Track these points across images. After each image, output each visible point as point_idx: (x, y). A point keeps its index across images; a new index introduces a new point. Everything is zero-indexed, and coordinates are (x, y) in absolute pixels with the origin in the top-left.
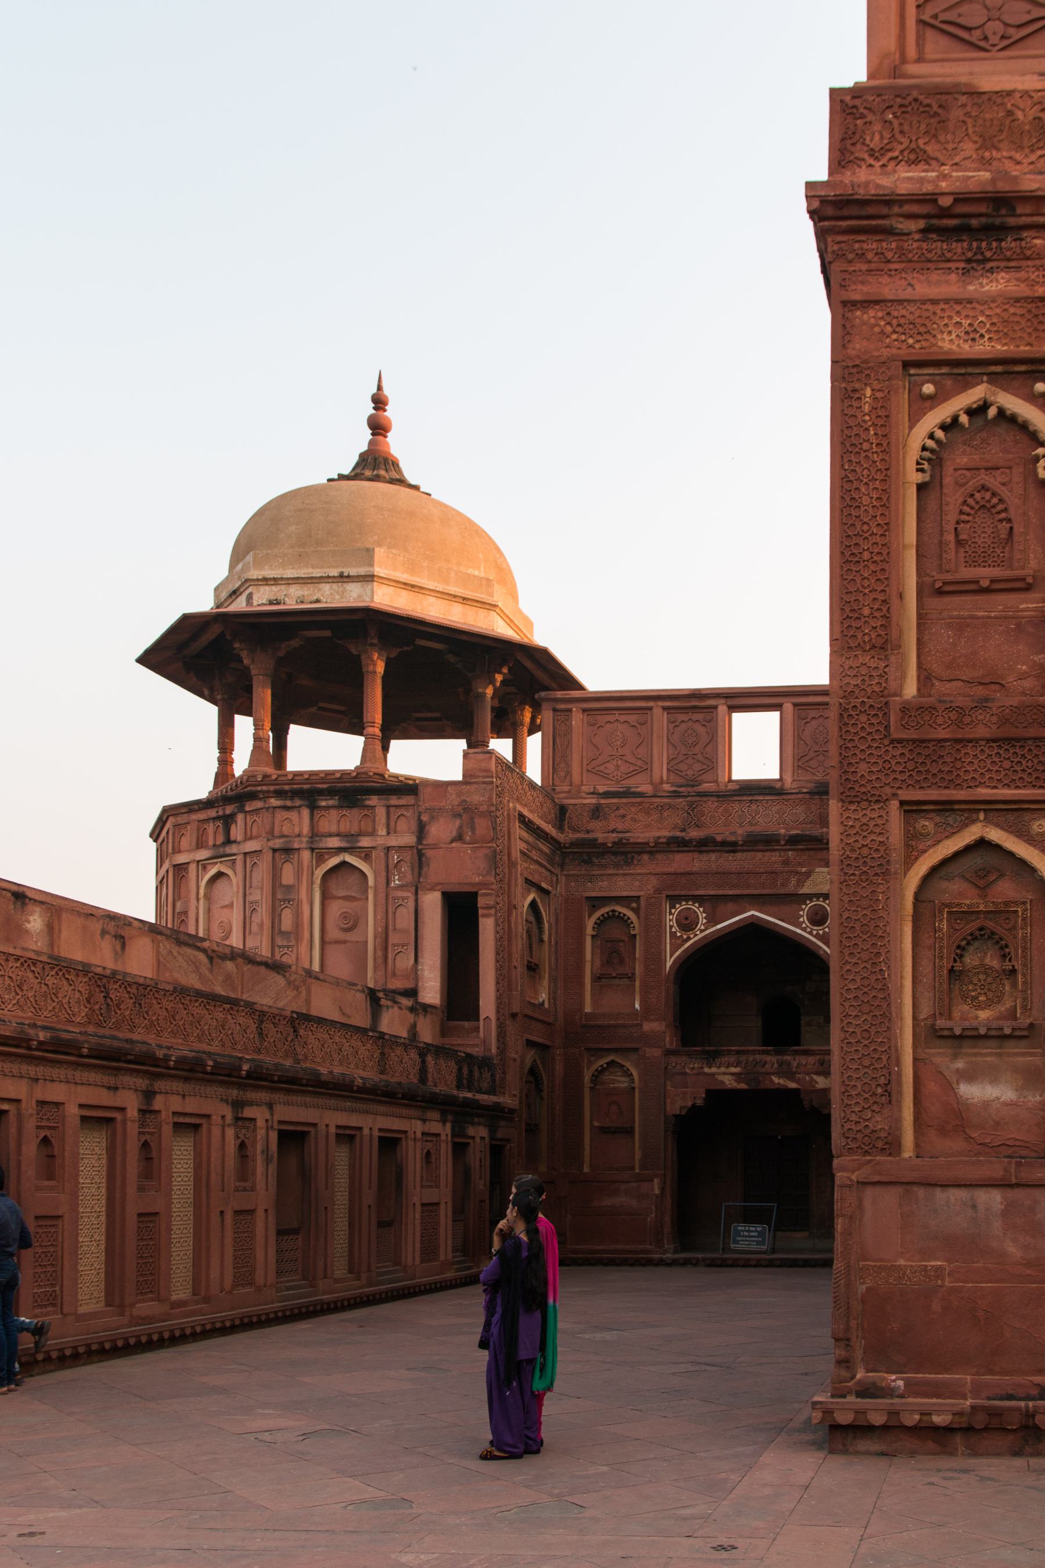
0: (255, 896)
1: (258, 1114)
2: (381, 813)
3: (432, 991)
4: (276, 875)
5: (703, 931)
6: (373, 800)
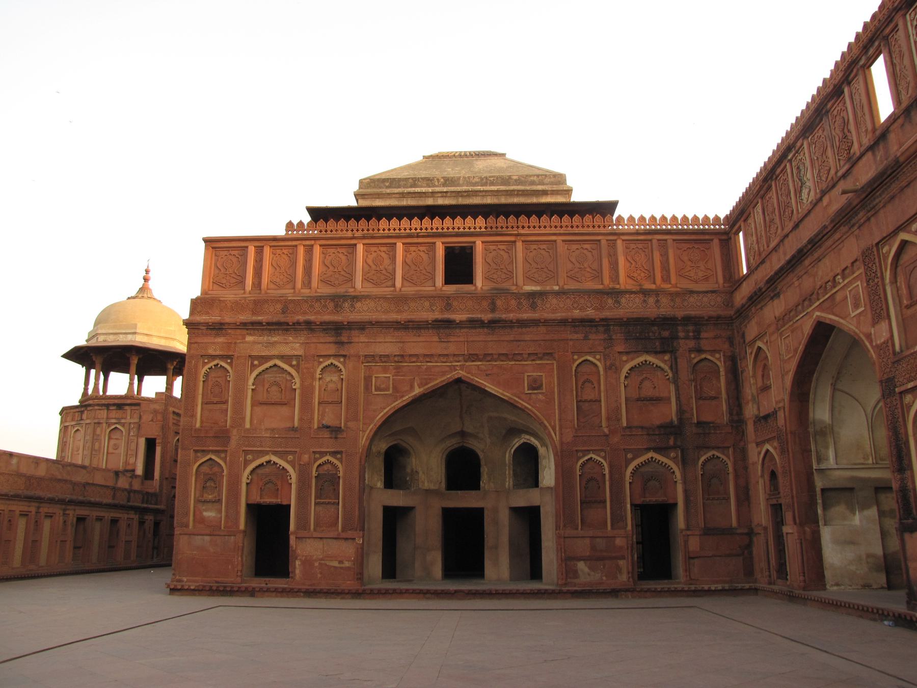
0: (88, 438)
1: (71, 513)
2: (129, 412)
6: (127, 407)
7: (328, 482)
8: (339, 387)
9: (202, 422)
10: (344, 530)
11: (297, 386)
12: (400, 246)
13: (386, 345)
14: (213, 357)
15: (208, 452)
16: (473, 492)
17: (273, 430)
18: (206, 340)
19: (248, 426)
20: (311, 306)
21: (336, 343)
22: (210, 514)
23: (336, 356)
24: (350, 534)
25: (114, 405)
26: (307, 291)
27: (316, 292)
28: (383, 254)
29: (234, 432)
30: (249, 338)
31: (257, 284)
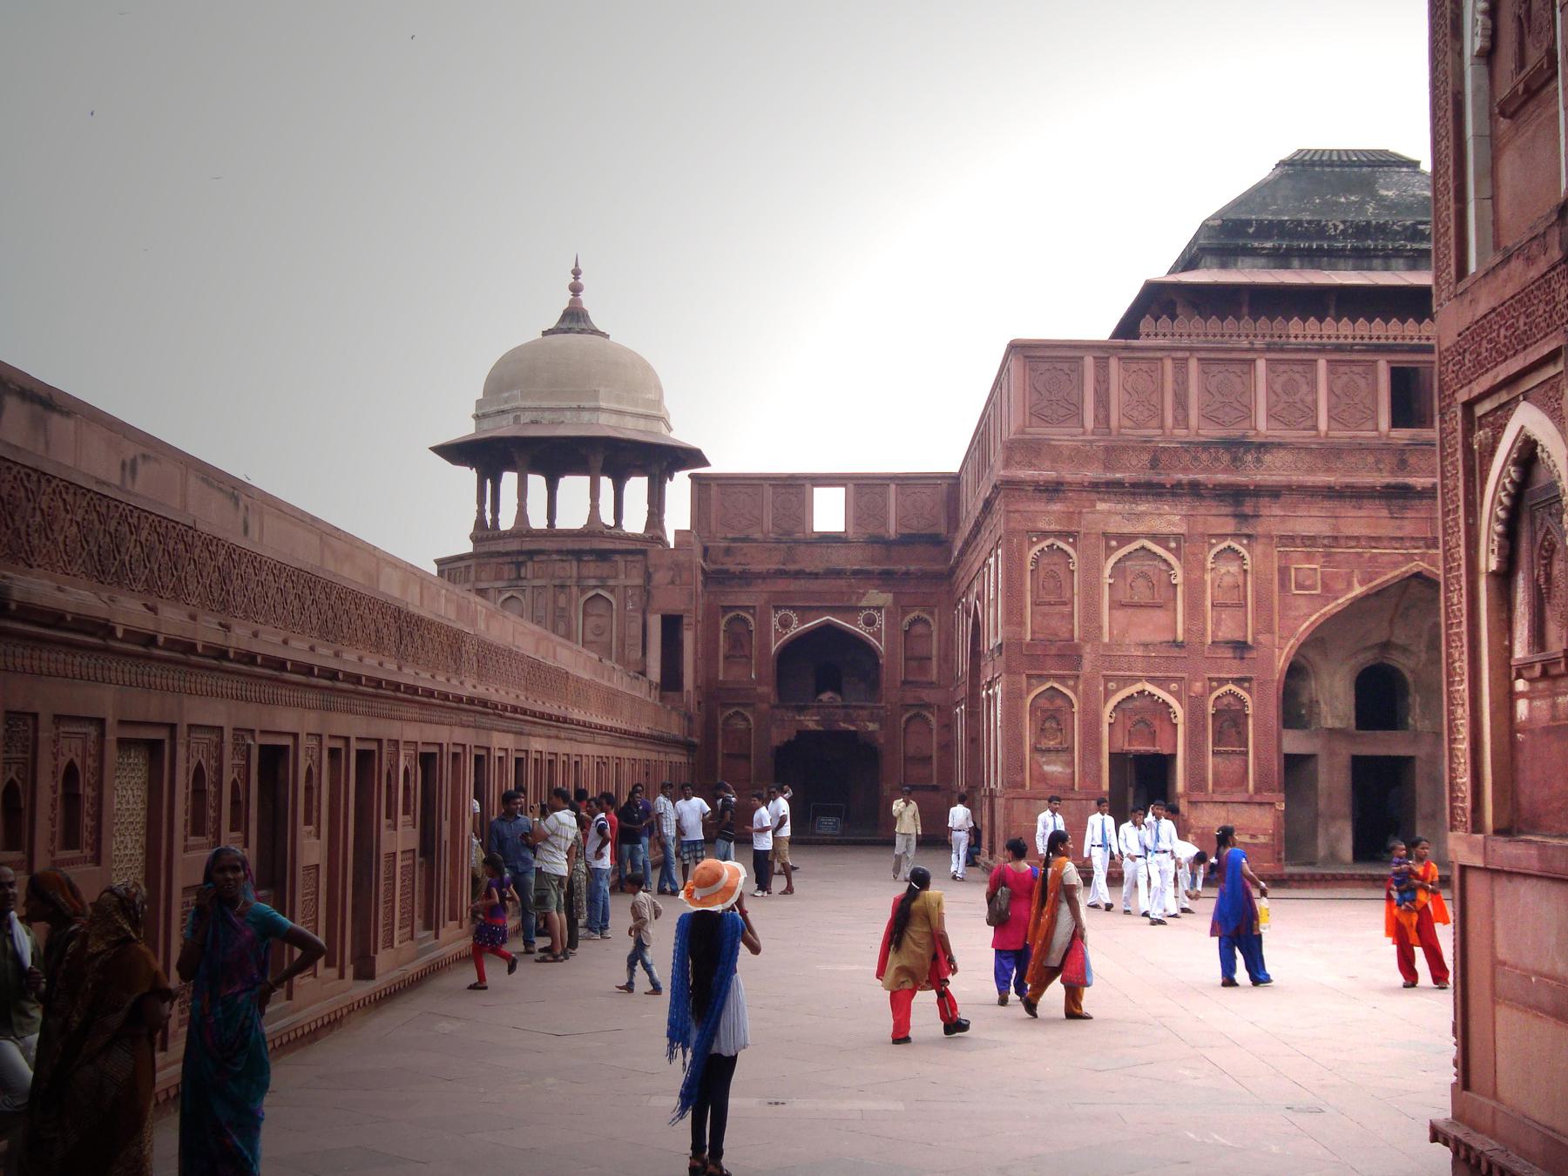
2: (621, 565)
3: (655, 672)
4: (555, 602)
5: (796, 628)
6: (617, 557)
7: (1230, 721)
8: (1240, 580)
9: (1033, 633)
10: (1258, 790)
11: (1178, 579)
12: (1322, 363)
13: (1311, 521)
14: (1045, 534)
15: (1049, 677)
16: (1398, 733)
17: (1146, 645)
18: (1033, 507)
19: (1106, 639)
20: (1196, 458)
21: (1235, 516)
22: (1054, 768)
23: (1235, 536)
24: (1267, 796)
25: (591, 552)
26: (1180, 432)
27: (1198, 434)
28: (1297, 376)
29: (1088, 648)
30: (1101, 506)
31: (1103, 418)
